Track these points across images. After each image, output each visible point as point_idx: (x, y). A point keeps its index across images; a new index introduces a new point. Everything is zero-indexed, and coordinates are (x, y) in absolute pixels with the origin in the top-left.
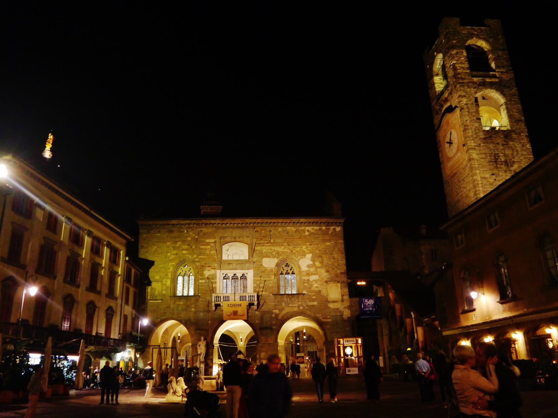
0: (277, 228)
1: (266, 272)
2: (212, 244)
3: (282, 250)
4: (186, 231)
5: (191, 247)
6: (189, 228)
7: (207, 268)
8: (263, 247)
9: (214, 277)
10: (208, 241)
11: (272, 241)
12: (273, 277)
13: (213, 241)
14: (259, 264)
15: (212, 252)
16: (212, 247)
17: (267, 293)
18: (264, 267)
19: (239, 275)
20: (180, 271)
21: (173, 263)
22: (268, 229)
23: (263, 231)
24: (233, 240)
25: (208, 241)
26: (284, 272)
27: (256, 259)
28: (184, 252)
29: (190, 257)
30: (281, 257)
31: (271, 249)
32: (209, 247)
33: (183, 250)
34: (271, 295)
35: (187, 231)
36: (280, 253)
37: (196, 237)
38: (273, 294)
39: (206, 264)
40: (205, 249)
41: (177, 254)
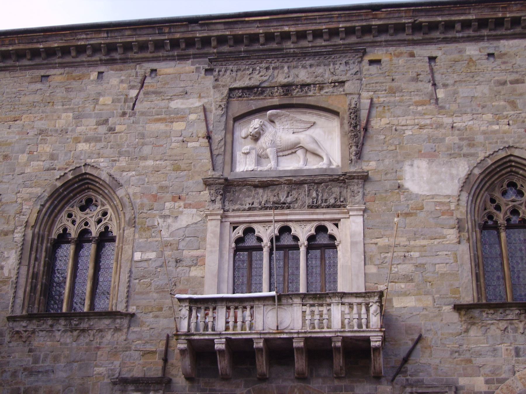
0: (461, 46)
1: (422, 215)
2: (192, 117)
3: (483, 128)
4: (94, 75)
5: (112, 130)
6: (112, 62)
7: (167, 205)
8: (402, 121)
9: (197, 236)
10: (176, 104)
11: (441, 94)
12: (452, 234)
13: (196, 103)
14: (388, 185)
15: (190, 145)
16: (190, 124)
17: (428, 301)
18: (409, 195)
19: (303, 233)
20: (63, 221)
21: (38, 190)
22: (424, 52)
23: (401, 61)
24: (276, 101)
25: (176, 104)
26: (501, 218)
27: (373, 164)
28: (82, 146)
29: (103, 163)
30: (481, 156)
31: (440, 126)
32: (178, 126)
33: (77, 140)
34: (447, 309)
35: (100, 73)
36: (480, 138)
37: (133, 93)
38: (458, 308)
39: (163, 188)
40: (167, 135)
41: (53, 157)
